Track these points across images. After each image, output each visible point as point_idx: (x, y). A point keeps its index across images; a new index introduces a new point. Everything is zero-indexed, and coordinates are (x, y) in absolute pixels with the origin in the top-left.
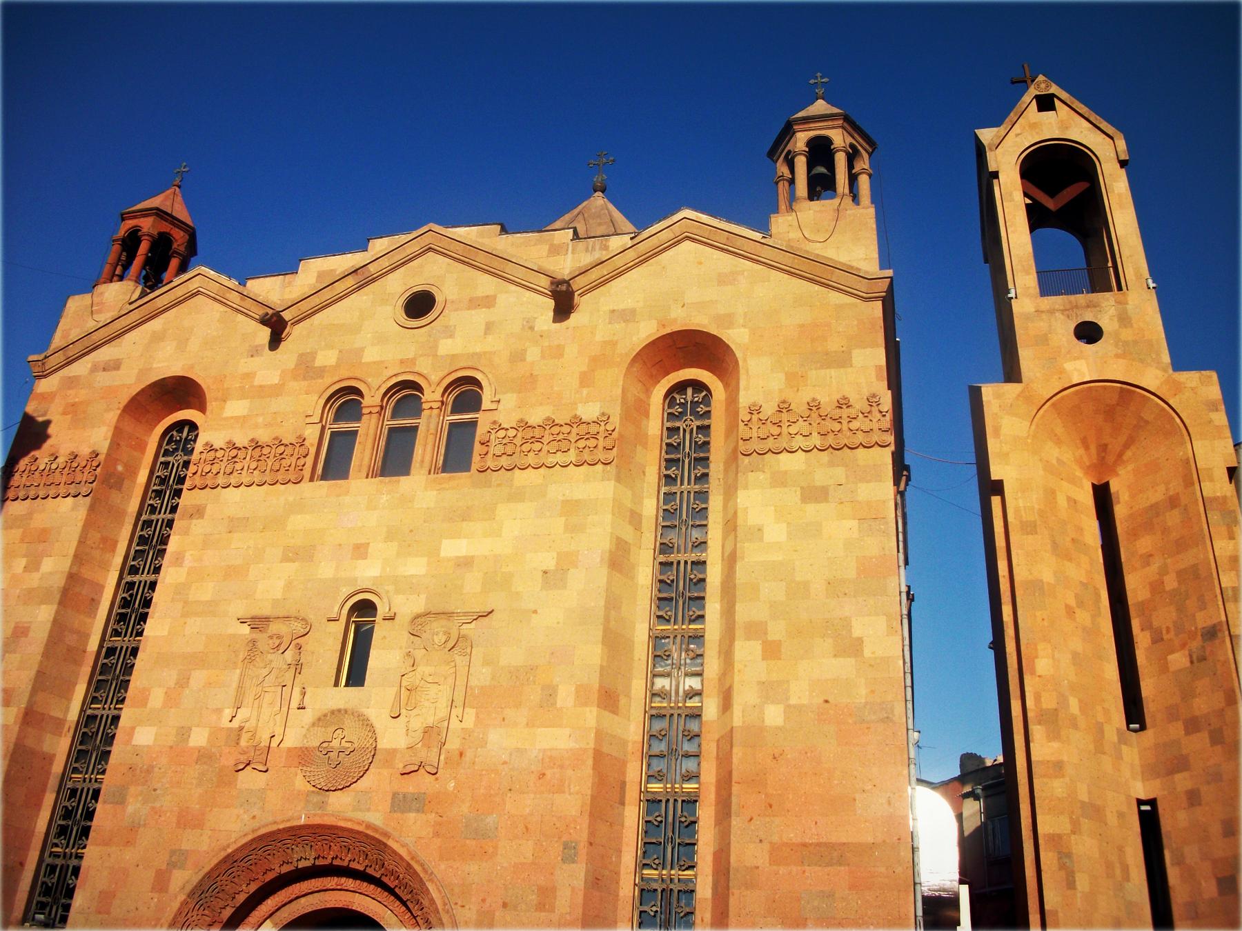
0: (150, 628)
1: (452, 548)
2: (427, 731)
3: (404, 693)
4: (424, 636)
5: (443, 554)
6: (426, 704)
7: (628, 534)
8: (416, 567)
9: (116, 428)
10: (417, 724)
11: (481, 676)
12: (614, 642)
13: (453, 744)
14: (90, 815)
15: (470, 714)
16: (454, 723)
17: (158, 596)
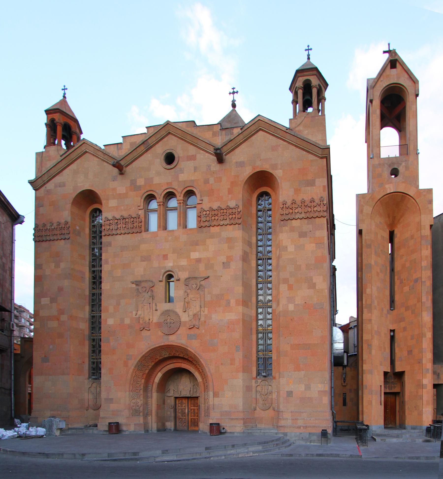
0: (103, 285)
1: (195, 255)
2: (194, 315)
3: (186, 304)
4: (189, 285)
5: (191, 258)
6: (193, 307)
7: (247, 249)
8: (184, 262)
9: (71, 212)
10: (191, 313)
11: (208, 298)
12: (246, 285)
13: (203, 319)
14: (100, 346)
15: (206, 309)
16: (202, 313)
17: (103, 275)
